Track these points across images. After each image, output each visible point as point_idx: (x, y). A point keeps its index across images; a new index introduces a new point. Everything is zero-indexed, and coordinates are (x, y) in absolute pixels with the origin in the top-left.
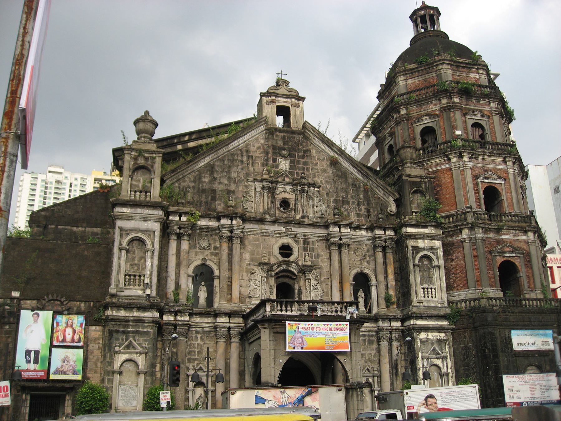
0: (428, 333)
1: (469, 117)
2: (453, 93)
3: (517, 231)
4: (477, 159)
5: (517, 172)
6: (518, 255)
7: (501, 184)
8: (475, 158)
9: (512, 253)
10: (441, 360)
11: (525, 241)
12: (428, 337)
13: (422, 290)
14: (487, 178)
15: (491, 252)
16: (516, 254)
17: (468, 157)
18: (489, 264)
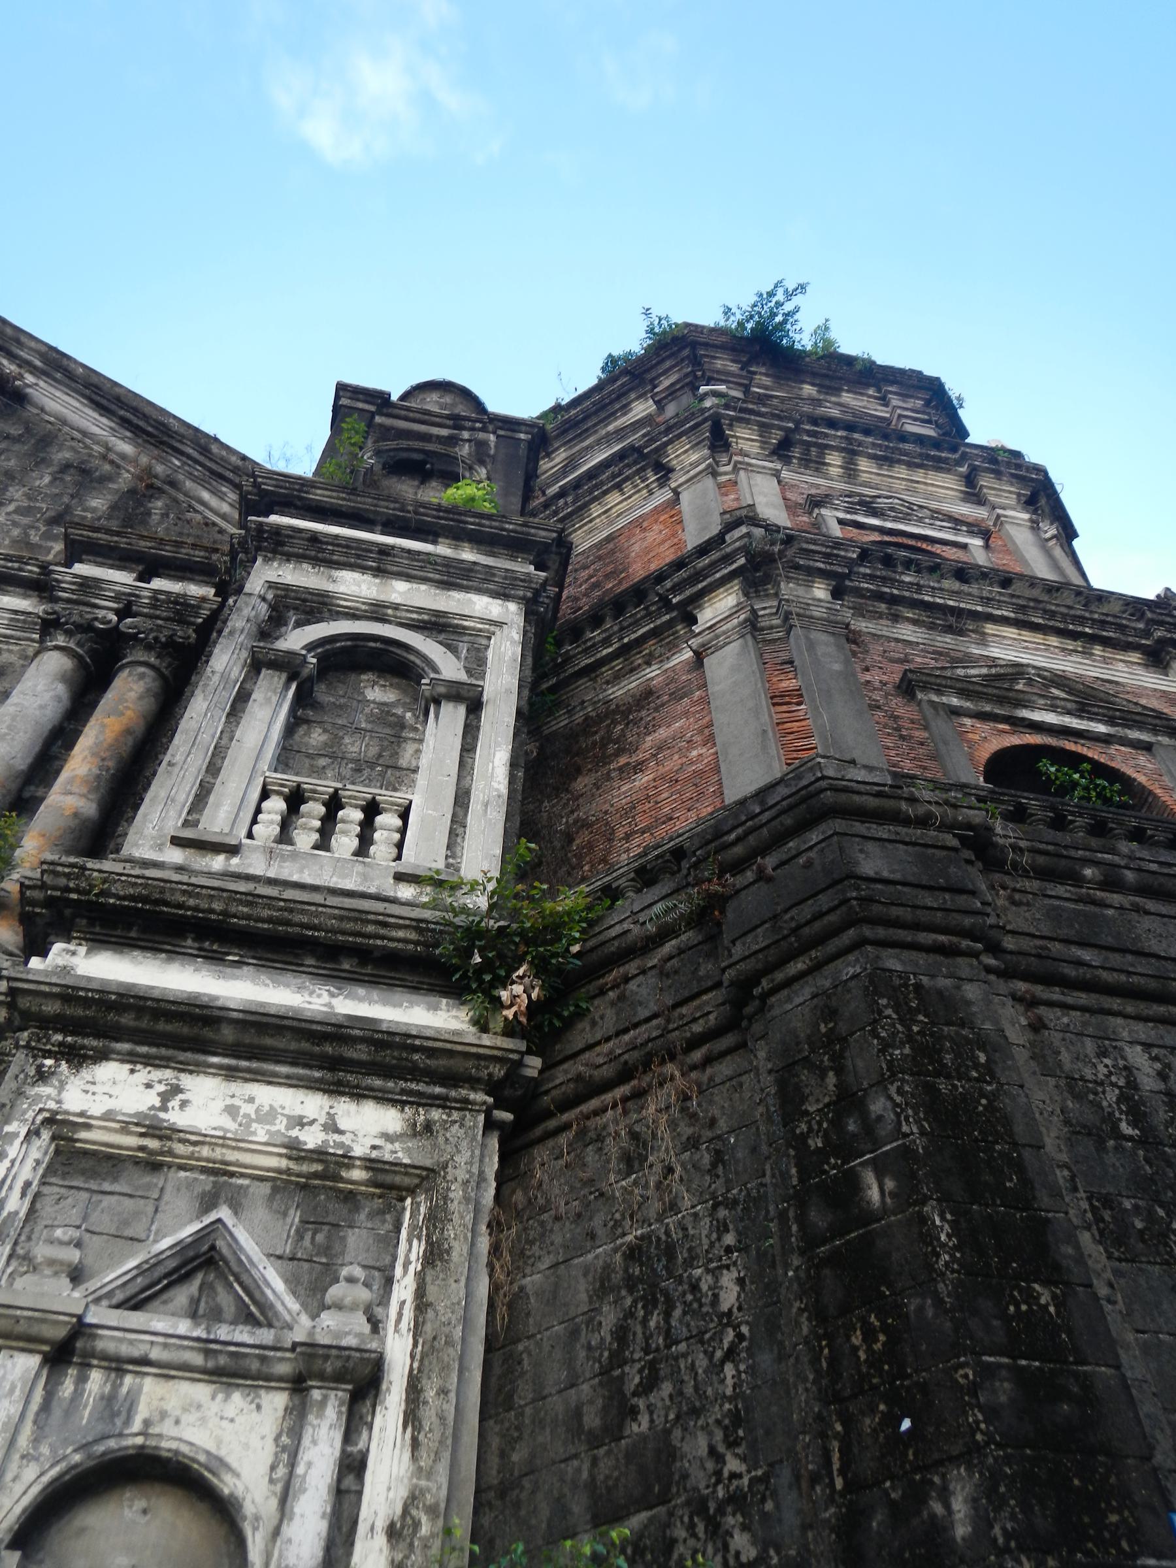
0: (186, 1080)
6: (1134, 734)
10: (277, 1401)
12: (175, 1117)
13: (275, 805)
14: (875, 513)
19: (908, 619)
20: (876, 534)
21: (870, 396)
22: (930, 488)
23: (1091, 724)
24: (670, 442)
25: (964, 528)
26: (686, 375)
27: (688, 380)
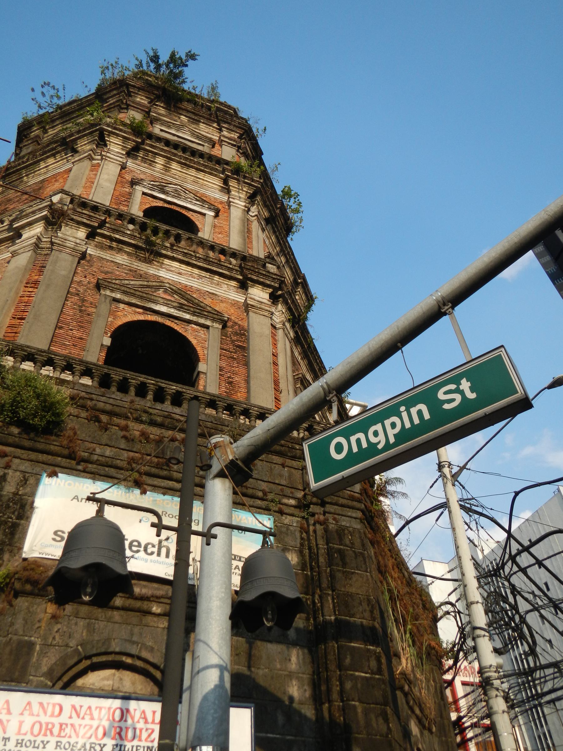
1: (163, 128)
2: (134, 86)
3: (216, 278)
4: (152, 163)
5: (256, 213)
6: (202, 321)
7: (204, 215)
8: (144, 160)
9: (180, 307)
11: (235, 304)
14: (164, 192)
15: (98, 287)
16: (194, 314)
17: (124, 148)
18: (81, 311)
19: (126, 252)
20: (162, 202)
21: (214, 127)
22: (205, 182)
23: (184, 314)
24: (79, 138)
25: (207, 206)
26: (117, 101)
27: (118, 104)
